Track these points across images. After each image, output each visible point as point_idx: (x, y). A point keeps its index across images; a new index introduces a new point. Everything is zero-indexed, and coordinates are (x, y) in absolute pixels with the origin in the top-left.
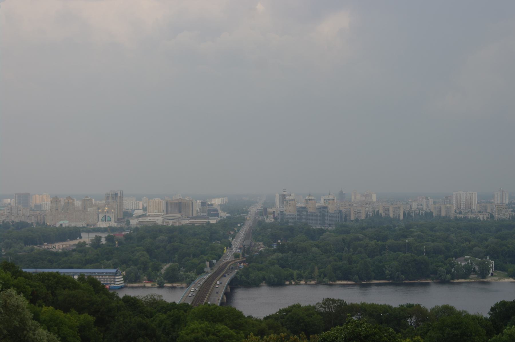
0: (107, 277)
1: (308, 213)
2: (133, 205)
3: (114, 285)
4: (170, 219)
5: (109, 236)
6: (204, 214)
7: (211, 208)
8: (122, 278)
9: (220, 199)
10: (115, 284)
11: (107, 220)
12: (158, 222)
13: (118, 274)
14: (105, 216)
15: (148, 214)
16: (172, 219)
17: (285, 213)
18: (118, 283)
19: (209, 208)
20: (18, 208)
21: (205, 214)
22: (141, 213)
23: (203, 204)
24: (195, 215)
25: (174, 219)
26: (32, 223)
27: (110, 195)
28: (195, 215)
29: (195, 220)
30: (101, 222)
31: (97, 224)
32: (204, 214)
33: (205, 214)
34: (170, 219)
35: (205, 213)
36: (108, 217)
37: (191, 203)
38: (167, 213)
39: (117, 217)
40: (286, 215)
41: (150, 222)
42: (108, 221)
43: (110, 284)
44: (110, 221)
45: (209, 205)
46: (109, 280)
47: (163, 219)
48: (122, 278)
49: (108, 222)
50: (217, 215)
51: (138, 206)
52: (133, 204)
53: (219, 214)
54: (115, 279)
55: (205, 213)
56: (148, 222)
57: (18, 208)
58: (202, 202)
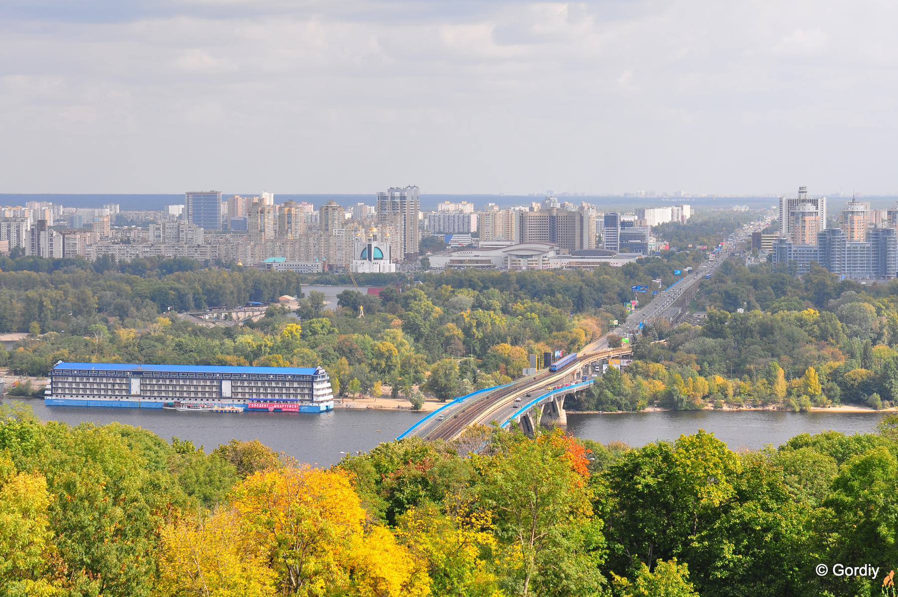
0: (296, 385)
1: (845, 244)
2: (456, 224)
3: (311, 404)
4: (522, 256)
5: (346, 293)
6: (611, 245)
7: (628, 230)
8: (330, 388)
9: (670, 209)
10: (312, 401)
11: (373, 259)
12: (494, 262)
13: (318, 379)
14: (370, 246)
15: (481, 243)
16: (527, 256)
17: (790, 244)
18: (321, 399)
19: (624, 231)
20: (179, 226)
21: (614, 245)
22: (466, 240)
23: (611, 221)
24: (586, 247)
25: (531, 256)
26: (206, 261)
27: (389, 198)
28: (586, 247)
29: (582, 258)
30: (360, 262)
31: (351, 265)
32: (611, 245)
33: (614, 245)
34: (522, 256)
35: (614, 242)
36: (376, 249)
37: (577, 218)
38: (522, 241)
39: (405, 249)
40: (793, 249)
41: (477, 262)
42: (375, 259)
43: (302, 401)
44: (382, 259)
45: (624, 224)
46: (299, 391)
47: (505, 254)
48: (330, 388)
49: (376, 261)
50: (643, 247)
51: (466, 226)
52: (456, 220)
53: (647, 244)
54: (312, 389)
55: (614, 242)
56: (471, 261)
57: (179, 226)
58: (606, 218)
